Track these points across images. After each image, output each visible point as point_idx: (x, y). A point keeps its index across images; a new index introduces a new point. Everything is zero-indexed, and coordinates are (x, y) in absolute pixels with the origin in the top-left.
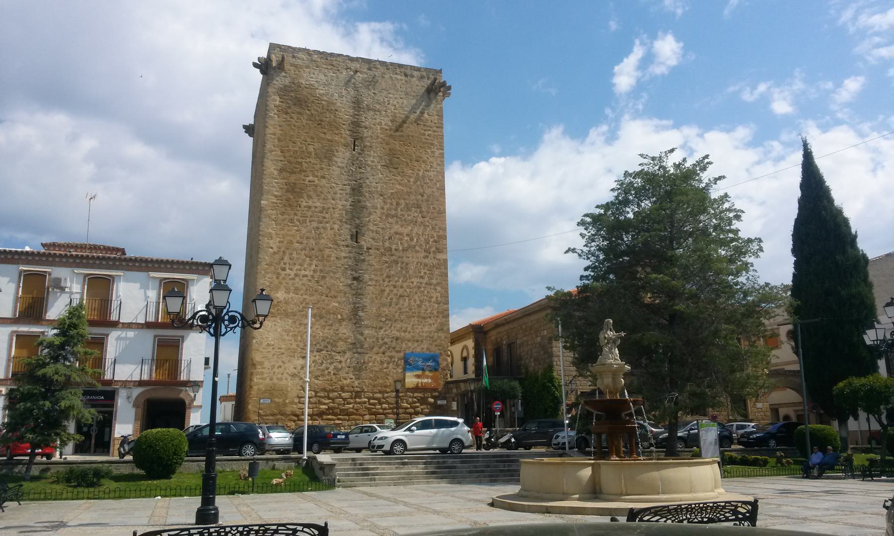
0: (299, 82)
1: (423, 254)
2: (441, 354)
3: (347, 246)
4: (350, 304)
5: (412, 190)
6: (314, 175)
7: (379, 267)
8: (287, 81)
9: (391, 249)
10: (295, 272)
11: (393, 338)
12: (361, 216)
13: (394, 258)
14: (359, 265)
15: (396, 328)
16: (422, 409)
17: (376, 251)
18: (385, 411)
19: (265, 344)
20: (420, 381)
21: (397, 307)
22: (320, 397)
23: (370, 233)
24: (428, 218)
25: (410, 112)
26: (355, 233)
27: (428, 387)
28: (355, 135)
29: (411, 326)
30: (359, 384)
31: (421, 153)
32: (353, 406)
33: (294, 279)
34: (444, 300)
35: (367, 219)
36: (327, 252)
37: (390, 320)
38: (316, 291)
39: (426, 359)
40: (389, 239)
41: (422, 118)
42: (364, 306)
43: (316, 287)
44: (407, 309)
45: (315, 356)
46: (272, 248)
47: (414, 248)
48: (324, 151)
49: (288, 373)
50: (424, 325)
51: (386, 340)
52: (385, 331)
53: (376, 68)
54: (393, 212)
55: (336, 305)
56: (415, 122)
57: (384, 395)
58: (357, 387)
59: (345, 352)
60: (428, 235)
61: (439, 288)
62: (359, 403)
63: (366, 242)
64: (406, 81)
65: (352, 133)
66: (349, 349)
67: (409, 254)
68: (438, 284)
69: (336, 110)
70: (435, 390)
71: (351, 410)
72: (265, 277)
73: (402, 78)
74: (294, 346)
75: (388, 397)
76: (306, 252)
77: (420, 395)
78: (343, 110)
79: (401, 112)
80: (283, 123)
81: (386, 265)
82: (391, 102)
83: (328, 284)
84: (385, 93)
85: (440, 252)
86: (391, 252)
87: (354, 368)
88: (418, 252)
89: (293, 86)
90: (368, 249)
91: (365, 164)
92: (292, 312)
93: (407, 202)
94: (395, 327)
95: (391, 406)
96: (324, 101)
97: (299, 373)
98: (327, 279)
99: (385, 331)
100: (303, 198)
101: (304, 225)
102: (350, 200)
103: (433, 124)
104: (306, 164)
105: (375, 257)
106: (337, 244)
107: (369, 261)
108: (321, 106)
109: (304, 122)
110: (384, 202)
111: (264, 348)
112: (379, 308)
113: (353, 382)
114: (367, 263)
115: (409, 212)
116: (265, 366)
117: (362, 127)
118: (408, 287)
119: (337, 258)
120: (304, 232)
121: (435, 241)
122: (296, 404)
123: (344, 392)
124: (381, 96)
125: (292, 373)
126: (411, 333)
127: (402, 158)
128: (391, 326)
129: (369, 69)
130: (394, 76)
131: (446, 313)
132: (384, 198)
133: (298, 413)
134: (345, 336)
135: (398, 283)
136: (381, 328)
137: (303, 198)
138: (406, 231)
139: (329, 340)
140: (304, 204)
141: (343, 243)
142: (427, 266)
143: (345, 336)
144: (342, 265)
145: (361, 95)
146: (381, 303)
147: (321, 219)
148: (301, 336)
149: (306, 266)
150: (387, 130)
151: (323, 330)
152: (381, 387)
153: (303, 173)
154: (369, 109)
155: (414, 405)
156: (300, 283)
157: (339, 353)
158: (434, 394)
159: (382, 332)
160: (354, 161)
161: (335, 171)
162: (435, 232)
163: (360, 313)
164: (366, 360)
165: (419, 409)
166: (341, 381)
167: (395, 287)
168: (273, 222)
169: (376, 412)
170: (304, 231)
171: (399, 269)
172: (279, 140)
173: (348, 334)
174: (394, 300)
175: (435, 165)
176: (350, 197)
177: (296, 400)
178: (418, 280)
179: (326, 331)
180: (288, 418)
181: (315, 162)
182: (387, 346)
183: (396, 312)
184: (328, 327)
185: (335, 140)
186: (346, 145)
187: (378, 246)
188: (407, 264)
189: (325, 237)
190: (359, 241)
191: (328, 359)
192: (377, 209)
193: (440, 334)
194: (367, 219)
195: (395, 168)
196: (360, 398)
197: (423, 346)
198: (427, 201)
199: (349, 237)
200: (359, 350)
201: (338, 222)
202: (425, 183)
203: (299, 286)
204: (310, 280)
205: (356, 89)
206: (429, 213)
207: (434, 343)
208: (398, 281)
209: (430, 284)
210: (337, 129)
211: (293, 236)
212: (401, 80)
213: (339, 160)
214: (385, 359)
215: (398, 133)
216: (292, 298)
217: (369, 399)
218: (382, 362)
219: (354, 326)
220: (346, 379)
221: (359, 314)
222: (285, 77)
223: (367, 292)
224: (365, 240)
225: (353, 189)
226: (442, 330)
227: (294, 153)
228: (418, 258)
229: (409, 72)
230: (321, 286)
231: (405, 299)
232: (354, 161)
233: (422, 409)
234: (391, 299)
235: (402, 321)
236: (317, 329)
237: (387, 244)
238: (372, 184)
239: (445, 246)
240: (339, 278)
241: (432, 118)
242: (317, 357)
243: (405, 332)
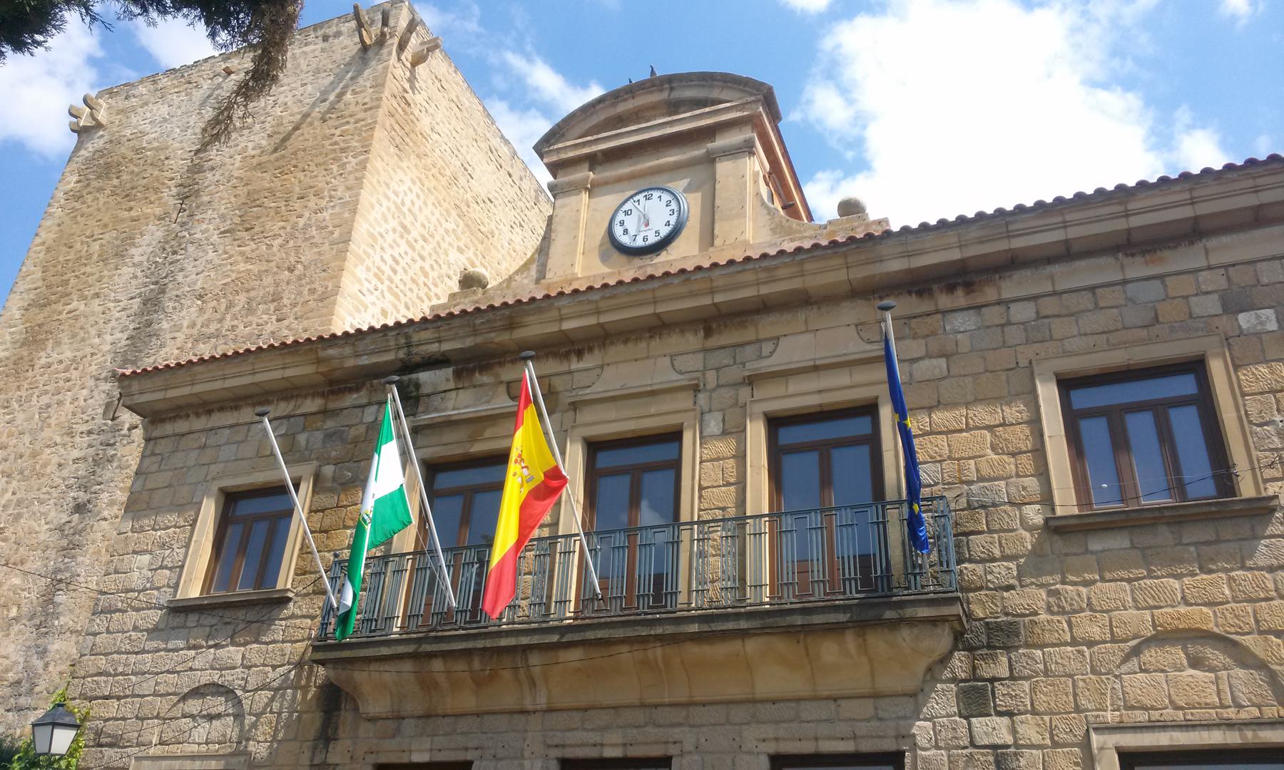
69: (167, 158)
144: (64, 479)
161: (127, 271)
172: (48, 250)
232: (167, 242)
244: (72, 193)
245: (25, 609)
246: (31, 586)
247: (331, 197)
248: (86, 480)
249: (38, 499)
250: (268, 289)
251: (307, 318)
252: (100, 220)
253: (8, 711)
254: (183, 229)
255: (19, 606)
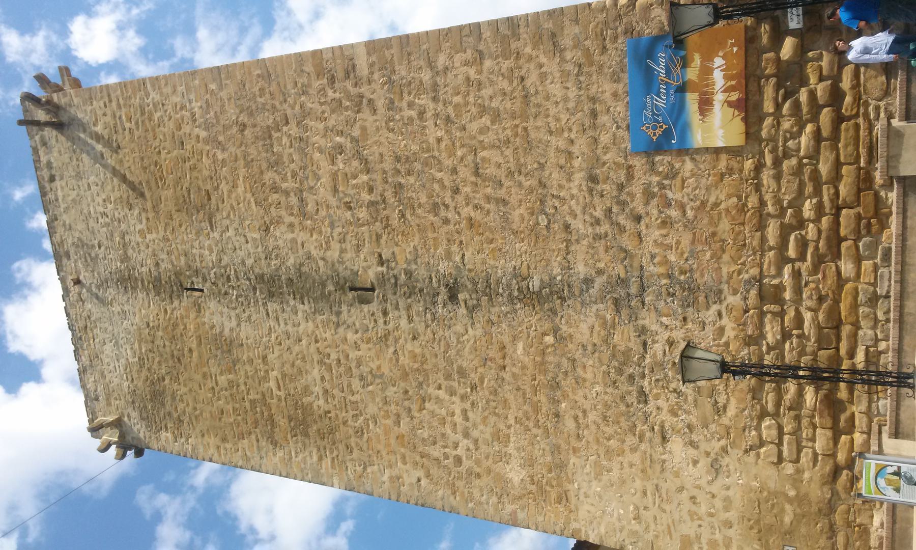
0: (129, 393)
1: (366, 114)
2: (629, 31)
3: (385, 313)
4: (515, 311)
5: (239, 152)
6: (266, 378)
7: (417, 235)
8: (135, 414)
9: (372, 204)
10: (459, 437)
11: (590, 191)
12: (317, 277)
13: (389, 194)
14: (419, 285)
15: (564, 182)
16: (821, 79)
17: (383, 241)
18: (827, 210)
19: (635, 526)
20: (719, 98)
21: (507, 183)
22: (778, 404)
23: (348, 256)
24: (285, 106)
25: (105, 166)
26: (355, 294)
27: (742, 65)
28: (175, 288)
29: (553, 139)
30: (735, 292)
31: (164, 135)
32: (809, 309)
33: (476, 441)
34: (471, 39)
35: (321, 263)
36: (404, 360)
37: (542, 202)
38: (495, 392)
39: (648, 78)
40: (350, 208)
41: (106, 137)
42: (515, 276)
43: (487, 393)
44: (508, 152)
45: (658, 408)
46: (419, 480)
47: (357, 141)
48: (219, 352)
49: (710, 483)
50: (547, 98)
51: (599, 213)
52: (575, 216)
53: (62, 242)
54: (294, 200)
55: (520, 346)
56: (117, 153)
57: (769, 214)
58: (745, 299)
59: (643, 331)
60: (321, 104)
61: (442, 60)
62: (798, 291)
63: (369, 267)
64: (62, 178)
65: (174, 296)
66: (634, 317)
67: (372, 152)
68: (431, 64)
69: (148, 326)
70: (750, 39)
71: (821, 317)
72: (481, 503)
73: (59, 187)
74: (636, 458)
75: (778, 201)
76: (415, 407)
77: (769, 91)
78: (143, 311)
79: (109, 187)
80: (198, 430)
81: (408, 216)
82: (101, 209)
83: (476, 363)
84: (92, 223)
85: (354, 67)
86: (377, 203)
87: (685, 305)
88: (364, 129)
89: (137, 405)
90: (381, 262)
91: (220, 267)
92: (552, 454)
93: (264, 166)
94: (561, 187)
95: (809, 189)
96: (141, 349)
97: (708, 454)
98: (465, 365)
99: (575, 216)
100: (311, 404)
101: (361, 406)
102: (292, 303)
103: (109, 112)
104: (251, 391)
105: (397, 245)
106: (386, 336)
107: (408, 262)
108: (150, 355)
109: (184, 390)
110: (278, 222)
111: (647, 530)
112: (515, 233)
113: (730, 310)
114: (414, 267)
115: (285, 159)
116: (693, 535)
117: (160, 273)
118: (451, 154)
119: (414, 338)
120: (376, 409)
121: (332, 80)
122: (799, 471)
123: (762, 336)
124: (99, 231)
125: (708, 472)
126: (572, 136)
127: (186, 185)
128: (558, 197)
129: (68, 255)
130: (63, 206)
131: (504, 30)
132: (271, 223)
133: (828, 469)
134: (597, 328)
135: (447, 183)
136: (567, 227)
137: (311, 404)
138: (325, 167)
139: (612, 371)
140: (321, 402)
141: (381, 321)
142: (392, 102)
143: (597, 328)
144: (427, 326)
145: (111, 273)
146: (503, 228)
147: (342, 369)
148: (609, 439)
149: (443, 412)
150: (148, 219)
151: (587, 384)
152: (743, 224)
153: (269, 401)
154: (125, 259)
155: (805, 109)
156: (481, 427)
157: (645, 344)
158: (765, 39)
159: (577, 224)
160: (220, 292)
161: (246, 332)
162: (309, 85)
163: (535, 284)
164: (661, 270)
165: (821, 90)
166: (727, 344)
167: (456, 191)
168: (369, 470)
169: (828, 239)
170: (372, 409)
171: (412, 180)
172: (224, 440)
173: (592, 320)
174: (489, 190)
175: (177, 99)
176: (288, 302)
177: (789, 469)
178: (430, 123)
179: (589, 376)
180: (843, 496)
181: (242, 373)
182: (615, 209)
183: (520, 185)
184: (580, 371)
185: (195, 332)
186: (199, 308)
187: (371, 237)
188: (398, 159)
189: (378, 363)
190: (369, 286)
191: (666, 375)
192: (294, 241)
193: (566, 41)
194: (321, 263)
195: (209, 199)
196: (780, 288)
197: (608, 95)
198: (251, 114)
199: (366, 308)
200: (633, 290)
201: (341, 330)
202: (218, 122)
203: (489, 430)
204: (473, 404)
205: (105, 284)
206: (274, 107)
207: (596, 58)
208: (441, 181)
209: (435, 87)
210: (177, 325)
211: (387, 433)
212: (62, 188)
213: (228, 325)
214: (655, 212)
215: (148, 195)
216: (518, 449)
217: (783, 260)
218: (664, 224)
219: (569, 302)
220: (722, 330)
221: (536, 289)
222: (129, 416)
223: (479, 267)
224: (365, 270)
225: (271, 295)
226: (554, 35)
227: (239, 415)
228: (378, 129)
229: (45, 174)
230: (482, 380)
231: (484, 159)
232: (220, 292)
233: (821, 79)
234: (488, 199)
235: (542, 166)
236: (586, 398)
237: (363, 214)
238: (251, 251)
239: (337, 53)
240: (459, 336)
241: (100, 113)
242: (660, 403)
243: (570, 155)
244: (176, 432)
245: (547, 326)
246: (524, 327)
247: (181, 109)
248: (427, 298)
249: (445, 352)
250: (260, 149)
251: (285, 86)
252: (200, 386)
253: (643, 304)
254: (208, 278)
255: (544, 334)
